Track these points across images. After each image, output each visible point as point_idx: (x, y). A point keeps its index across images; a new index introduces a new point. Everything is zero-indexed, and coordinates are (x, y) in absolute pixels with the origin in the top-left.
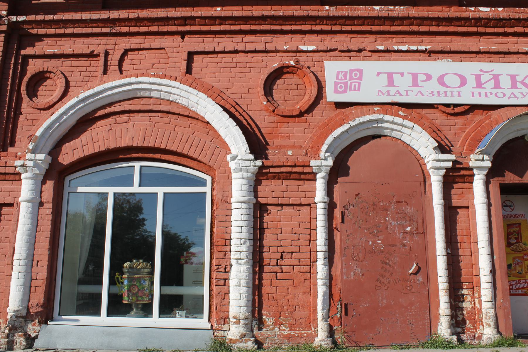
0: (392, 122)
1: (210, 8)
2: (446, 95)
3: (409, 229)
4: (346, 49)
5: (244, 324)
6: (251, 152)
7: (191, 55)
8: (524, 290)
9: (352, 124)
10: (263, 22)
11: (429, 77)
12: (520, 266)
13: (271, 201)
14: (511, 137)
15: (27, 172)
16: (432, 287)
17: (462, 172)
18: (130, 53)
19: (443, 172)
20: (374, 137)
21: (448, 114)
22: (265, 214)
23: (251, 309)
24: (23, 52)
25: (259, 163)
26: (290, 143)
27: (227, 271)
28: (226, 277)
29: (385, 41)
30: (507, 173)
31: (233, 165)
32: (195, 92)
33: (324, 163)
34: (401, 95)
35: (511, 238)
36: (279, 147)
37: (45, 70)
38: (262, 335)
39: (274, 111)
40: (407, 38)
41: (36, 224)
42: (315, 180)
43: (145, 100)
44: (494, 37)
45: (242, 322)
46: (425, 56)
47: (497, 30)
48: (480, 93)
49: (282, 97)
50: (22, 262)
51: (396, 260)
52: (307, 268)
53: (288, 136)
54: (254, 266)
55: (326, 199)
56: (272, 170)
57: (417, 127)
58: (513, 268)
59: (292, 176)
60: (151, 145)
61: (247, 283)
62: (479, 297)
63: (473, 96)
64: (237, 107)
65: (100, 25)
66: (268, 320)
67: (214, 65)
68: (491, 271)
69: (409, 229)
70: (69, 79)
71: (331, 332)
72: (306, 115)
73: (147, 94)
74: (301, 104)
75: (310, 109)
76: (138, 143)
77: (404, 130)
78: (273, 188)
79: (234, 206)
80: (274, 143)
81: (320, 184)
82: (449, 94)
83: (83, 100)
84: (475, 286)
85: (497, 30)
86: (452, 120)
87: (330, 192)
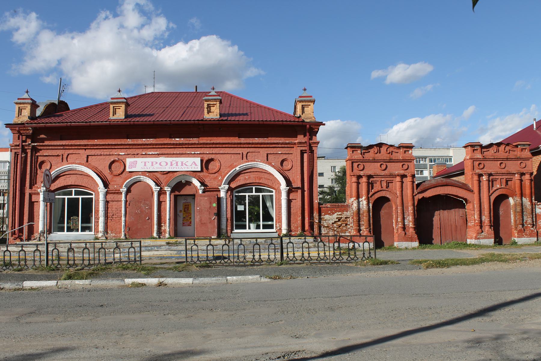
7: (88, 156)
9: (132, 178)
11: (157, 163)
13: (110, 200)
17: (163, 192)
20: (139, 181)
24: (36, 155)
25: (106, 190)
27: (98, 219)
30: (176, 192)
31: (99, 190)
32: (89, 169)
33: (124, 190)
36: (112, 185)
40: (152, 149)
46: (157, 156)
47: (180, 146)
50: (42, 218)
51: (143, 216)
52: (120, 218)
53: (115, 181)
54: (105, 218)
56: (110, 192)
60: (77, 184)
70: (52, 163)
71: (125, 235)
73: (75, 169)
75: (122, 173)
76: (73, 184)
78: (111, 196)
79: (100, 201)
80: (112, 183)
81: (123, 195)
82: (162, 168)
83: (56, 171)
84: (165, 223)
85: (180, 146)
87: (126, 198)
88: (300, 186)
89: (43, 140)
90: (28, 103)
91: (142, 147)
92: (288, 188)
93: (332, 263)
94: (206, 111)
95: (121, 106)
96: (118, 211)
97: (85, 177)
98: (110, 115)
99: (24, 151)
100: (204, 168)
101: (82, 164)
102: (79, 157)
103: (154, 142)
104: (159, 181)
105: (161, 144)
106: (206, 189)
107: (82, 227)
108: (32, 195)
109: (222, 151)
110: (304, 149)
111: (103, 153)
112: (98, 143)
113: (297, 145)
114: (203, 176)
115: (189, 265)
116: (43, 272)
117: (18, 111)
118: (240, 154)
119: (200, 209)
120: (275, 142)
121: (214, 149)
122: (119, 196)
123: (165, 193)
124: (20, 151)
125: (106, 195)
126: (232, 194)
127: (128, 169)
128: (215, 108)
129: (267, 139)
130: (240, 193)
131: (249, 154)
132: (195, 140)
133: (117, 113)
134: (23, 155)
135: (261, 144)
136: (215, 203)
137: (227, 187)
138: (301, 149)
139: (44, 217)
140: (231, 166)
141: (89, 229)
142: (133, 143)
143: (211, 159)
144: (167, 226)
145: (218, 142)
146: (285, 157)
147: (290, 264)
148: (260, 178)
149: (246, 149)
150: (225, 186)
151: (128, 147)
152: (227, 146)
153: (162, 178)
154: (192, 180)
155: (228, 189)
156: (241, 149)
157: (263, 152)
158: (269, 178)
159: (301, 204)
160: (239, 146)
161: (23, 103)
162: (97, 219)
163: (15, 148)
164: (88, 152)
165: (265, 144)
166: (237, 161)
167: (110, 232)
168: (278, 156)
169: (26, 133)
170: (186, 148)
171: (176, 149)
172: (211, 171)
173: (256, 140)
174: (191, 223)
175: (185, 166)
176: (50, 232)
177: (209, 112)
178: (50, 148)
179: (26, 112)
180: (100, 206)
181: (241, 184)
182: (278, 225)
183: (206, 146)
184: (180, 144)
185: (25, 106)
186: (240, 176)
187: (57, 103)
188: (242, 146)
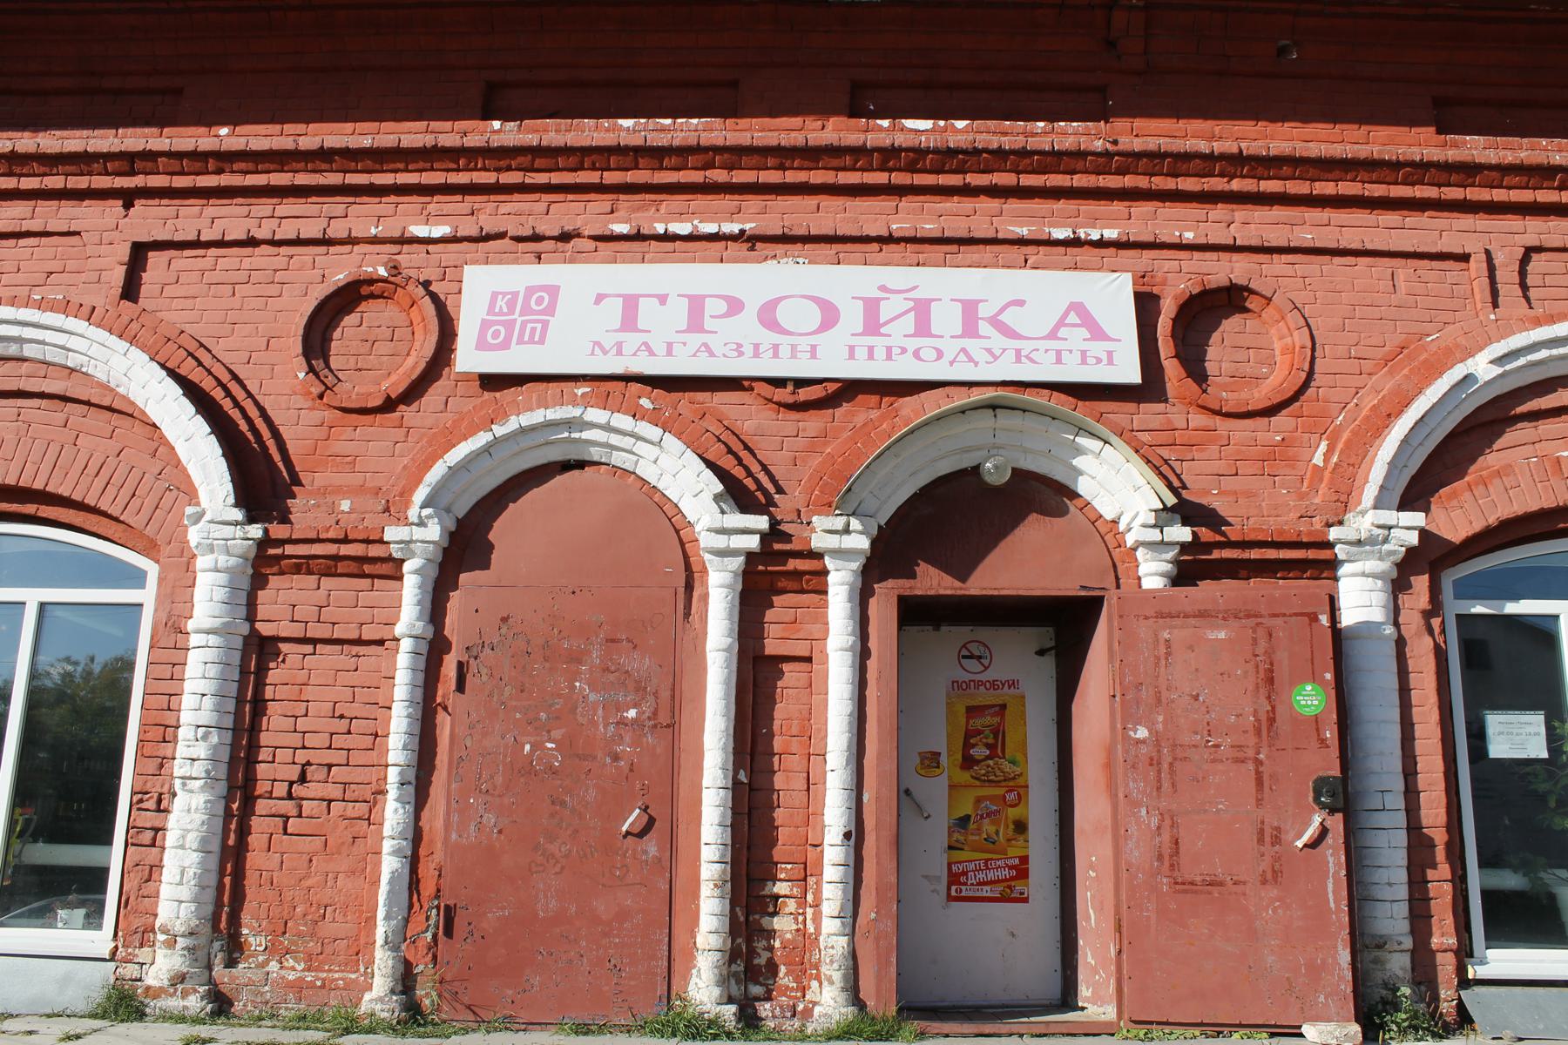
0: (607, 428)
1: (202, 130)
2: (776, 355)
3: (632, 713)
4: (528, 232)
5: (187, 948)
6: (237, 505)
7: (140, 253)
8: (1000, 887)
9: (499, 430)
10: (324, 166)
12: (993, 823)
13: (286, 629)
14: (945, 468)
17: (793, 564)
19: (738, 563)
20: (567, 466)
21: (779, 404)
22: (272, 665)
23: (209, 909)
26: (354, 479)
27: (161, 809)
28: (157, 824)
29: (639, 209)
31: (194, 535)
32: (123, 345)
33: (418, 533)
34: (652, 353)
35: (974, 746)
36: (324, 491)
38: (233, 979)
39: (321, 397)
40: (700, 202)
42: (400, 578)
44: (937, 198)
45: (182, 942)
48: (871, 349)
49: (353, 359)
51: (592, 795)
52: (362, 809)
53: (352, 462)
54: (229, 799)
55: (420, 627)
56: (290, 549)
57: (670, 441)
58: (972, 826)
61: (204, 841)
62: (817, 905)
63: (852, 356)
64: (233, 386)
66: (254, 941)
67: (195, 276)
68: (847, 836)
69: (632, 713)
71: (406, 981)
72: (402, 407)
74: (394, 378)
75: (414, 391)
77: (640, 447)
78: (293, 596)
79: (194, 640)
81: (411, 590)
82: (785, 351)
84: (807, 873)
86: (790, 422)
87: (436, 610)
96: (348, 742)
97: (97, 419)
100: (1171, 368)
101: (86, 310)
102: (71, 265)
104: (755, 468)
106: (1210, 546)
109: (1310, 227)
114: (1164, 437)
118: (1464, 258)
119: (1157, 739)
123: (815, 583)
125: (259, 581)
127: (469, 358)
130: (1516, 597)
131: (1537, 263)
136: (1315, 678)
137: (1407, 527)
143: (1219, 290)
149: (1513, 223)
150: (1390, 516)
152: (1348, 188)
154: (1078, 462)
164: (150, 221)
166: (1449, 317)
172: (1232, 399)
174: (1022, 872)
175: (998, 341)
180: (188, 686)
183: (1169, 184)
186: (1500, 443)
188: (1484, 195)
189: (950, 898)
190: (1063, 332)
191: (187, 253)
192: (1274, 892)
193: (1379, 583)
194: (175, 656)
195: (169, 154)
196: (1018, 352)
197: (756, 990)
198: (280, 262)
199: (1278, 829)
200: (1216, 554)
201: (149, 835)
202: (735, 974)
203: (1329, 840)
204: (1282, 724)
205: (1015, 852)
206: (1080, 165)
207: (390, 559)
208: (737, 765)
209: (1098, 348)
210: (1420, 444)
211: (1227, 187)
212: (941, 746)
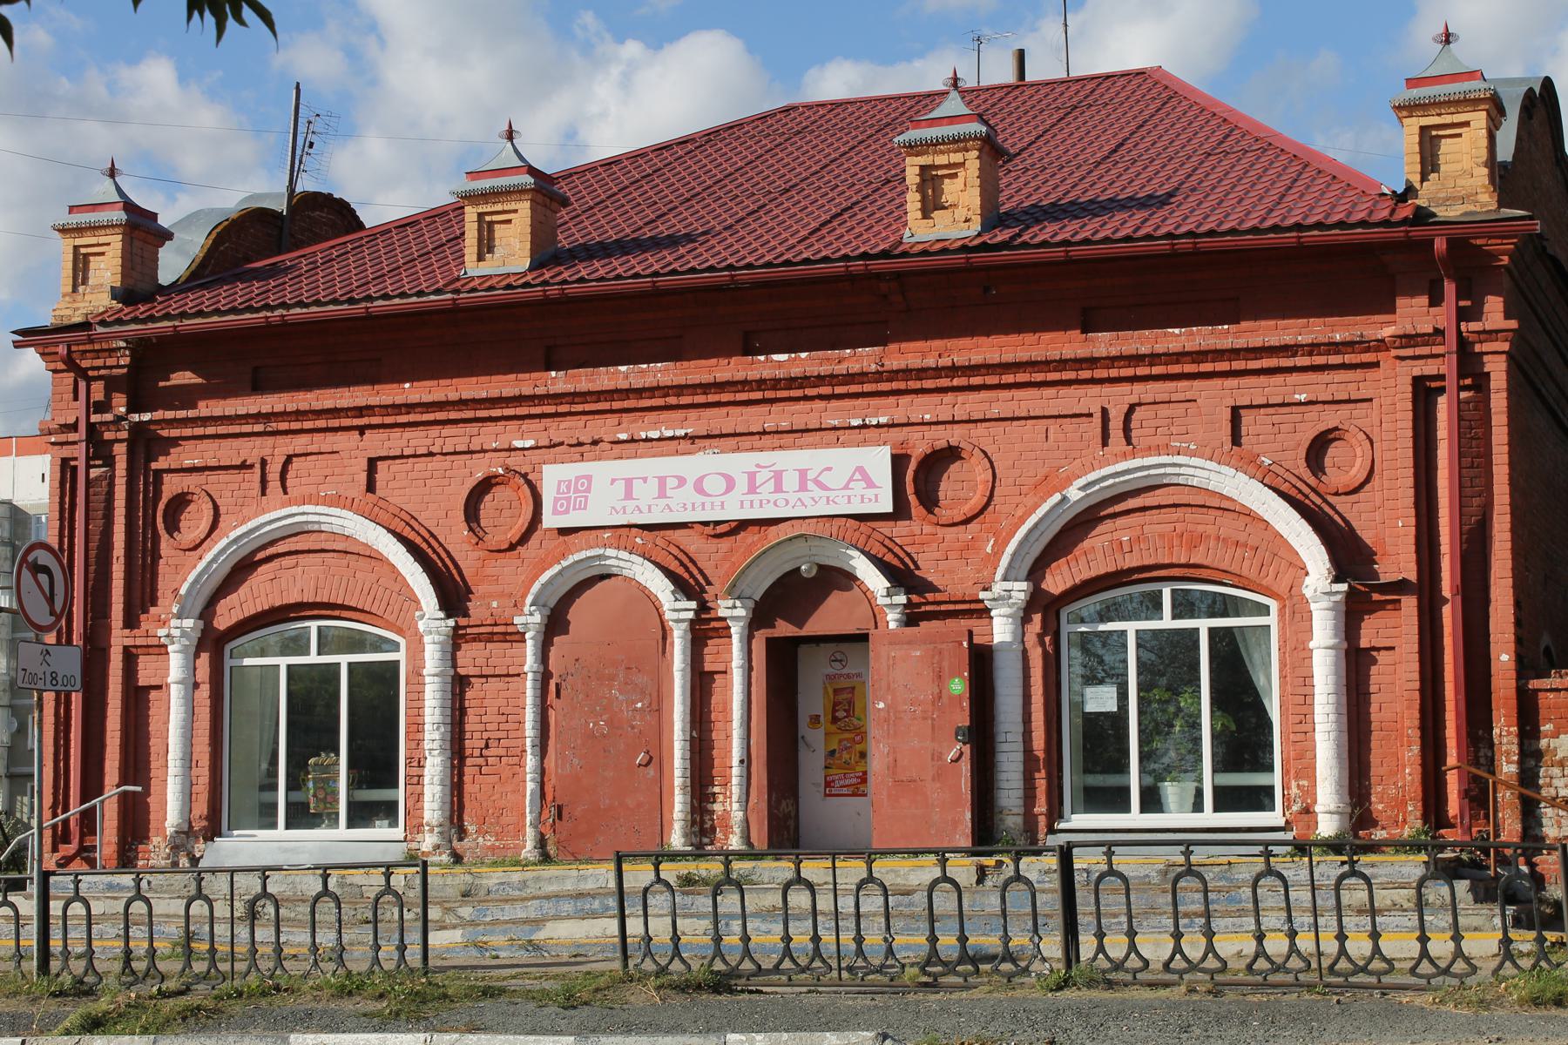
1: (395, 385)
2: (703, 509)
3: (639, 705)
4: (575, 442)
6: (440, 609)
7: (372, 464)
9: (565, 563)
10: (464, 408)
11: (682, 481)
12: (848, 753)
13: (471, 671)
15: (173, 643)
16: (665, 783)
17: (713, 624)
18: (294, 459)
19: (685, 625)
23: (448, 814)
24: (154, 466)
26: (499, 588)
29: (632, 422)
31: (421, 626)
33: (530, 619)
34: (641, 512)
35: (838, 711)
36: (483, 597)
37: (186, 491)
39: (477, 544)
40: (665, 415)
41: (191, 712)
42: (525, 641)
43: (315, 535)
44: (792, 403)
46: (685, 445)
48: (752, 502)
50: (178, 763)
52: (516, 760)
54: (452, 759)
56: (469, 631)
58: (837, 755)
59: (495, 638)
60: (325, 600)
61: (441, 780)
63: (742, 507)
64: (432, 541)
65: (250, 421)
66: (471, 828)
69: (639, 705)
70: (218, 501)
71: (542, 843)
72: (519, 547)
73: (316, 527)
74: (513, 531)
75: (524, 538)
76: (309, 597)
79: (428, 679)
81: (530, 648)
82: (708, 506)
83: (235, 541)
87: (544, 658)
88: (1412, 575)
89: (187, 397)
90: (113, 226)
91: (617, 405)
92: (1344, 587)
93: (1327, 985)
94: (913, 201)
95: (515, 211)
97: (362, 562)
98: (466, 258)
99: (99, 449)
100: (912, 498)
101: (349, 501)
102: (337, 471)
103: (665, 380)
104: (695, 572)
105: (705, 388)
106: (919, 605)
107: (351, 805)
108: (137, 656)
109: (1002, 403)
110: (1430, 368)
111: (439, 442)
112: (414, 398)
113: (1394, 352)
114: (908, 540)
115: (624, 982)
116: (14, 1001)
117: (70, 265)
118: (1091, 415)
120: (1273, 340)
121: (961, 397)
122: (511, 650)
123: (725, 633)
124: (80, 451)
125: (456, 647)
126: (1051, 629)
127: (551, 520)
128: (959, 181)
129: (1233, 328)
131: (1138, 414)
132: (863, 358)
133: (497, 242)
134: (94, 473)
135: (1200, 356)
136: (960, 675)
137: (1020, 590)
138: (1417, 372)
139: (189, 761)
140: (1049, 483)
141: (388, 811)
142: (570, 388)
143: (942, 450)
144: (735, 798)
145: (977, 359)
146: (1330, 418)
147: (1110, 985)
148: (1195, 541)
149: (1124, 388)
150: (1008, 585)
151: (551, 409)
152: (1022, 377)
153: (710, 556)
155: (1028, 602)
156: (1094, 390)
157: (1215, 397)
158: (1242, 538)
159: (1416, 676)
160: (1085, 374)
161: (93, 228)
162: (418, 763)
163: (62, 438)
164: (376, 443)
165: (1218, 354)
167: (471, 828)
168: (1293, 415)
169: (105, 367)
170: (821, 397)
171: (776, 408)
173: (1176, 338)
174: (864, 779)
176: (213, 831)
177: (931, 205)
178: (210, 430)
179: (107, 270)
180: (427, 703)
181: (1093, 573)
182: (1294, 791)
184: (791, 382)
185: (102, 240)
187: (281, 206)
189: (826, 795)
190: (852, 485)
191: (398, 461)
192: (938, 785)
193: (1010, 620)
194: (419, 688)
195: (380, 406)
196: (828, 498)
197: (706, 840)
198: (447, 464)
199: (941, 753)
200: (923, 609)
201: (416, 778)
202: (694, 833)
203: (963, 758)
204: (945, 699)
205: (859, 769)
206: (865, 379)
207: (518, 633)
208: (692, 728)
209: (870, 493)
210: (1037, 540)
211: (950, 384)
212: (821, 712)
